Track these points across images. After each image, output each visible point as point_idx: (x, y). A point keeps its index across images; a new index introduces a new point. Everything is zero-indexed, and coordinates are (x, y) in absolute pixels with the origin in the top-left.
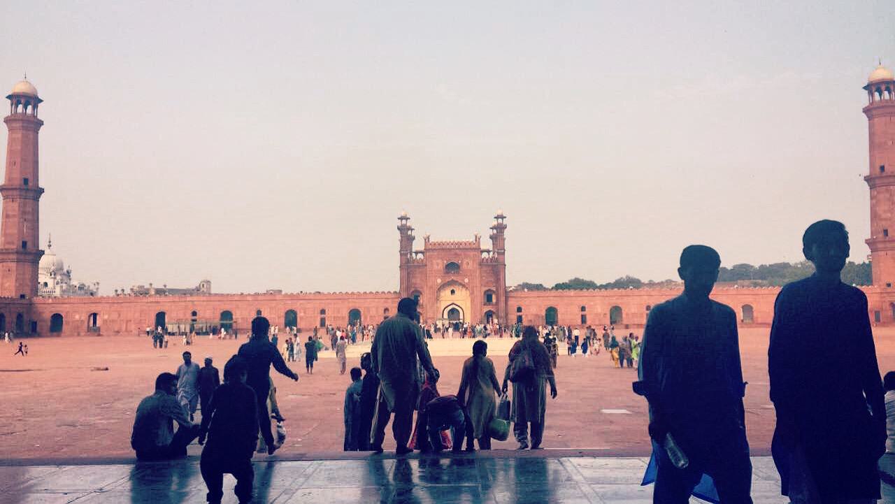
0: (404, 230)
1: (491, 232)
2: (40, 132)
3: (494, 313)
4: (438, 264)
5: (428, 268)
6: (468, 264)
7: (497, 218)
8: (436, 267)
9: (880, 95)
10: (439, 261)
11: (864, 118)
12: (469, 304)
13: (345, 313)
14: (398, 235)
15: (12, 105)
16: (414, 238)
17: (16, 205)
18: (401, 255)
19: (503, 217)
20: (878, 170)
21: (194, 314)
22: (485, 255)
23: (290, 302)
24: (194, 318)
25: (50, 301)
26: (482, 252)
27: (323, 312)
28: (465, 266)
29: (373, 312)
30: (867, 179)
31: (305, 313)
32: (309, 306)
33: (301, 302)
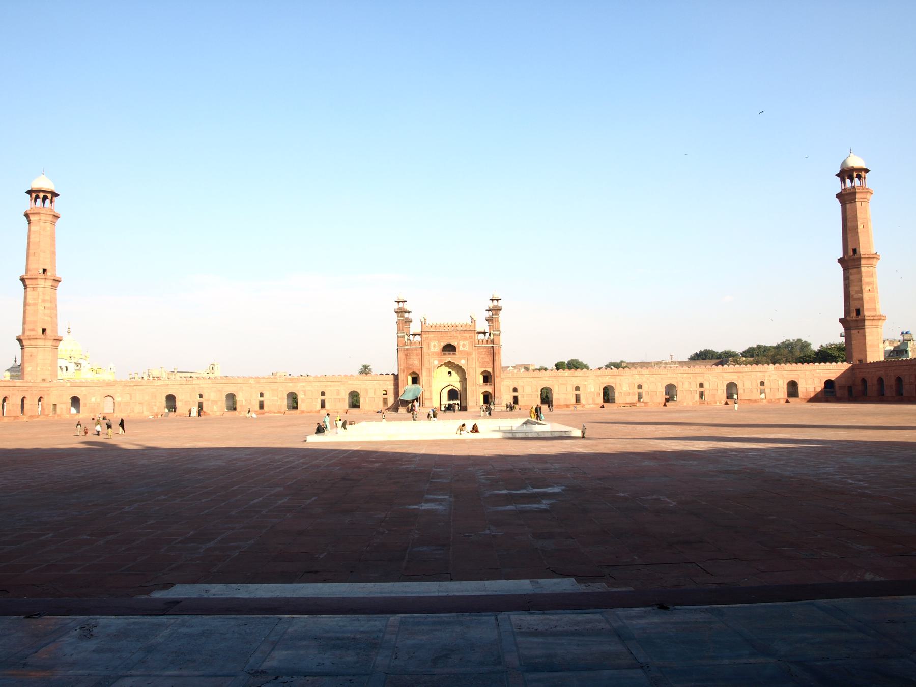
0: (400, 312)
4: (436, 346)
5: (425, 350)
6: (462, 345)
8: (433, 349)
10: (436, 343)
11: (838, 205)
18: (398, 337)
20: (851, 253)
23: (291, 384)
25: (69, 384)
27: (323, 394)
30: (840, 261)
32: (308, 388)
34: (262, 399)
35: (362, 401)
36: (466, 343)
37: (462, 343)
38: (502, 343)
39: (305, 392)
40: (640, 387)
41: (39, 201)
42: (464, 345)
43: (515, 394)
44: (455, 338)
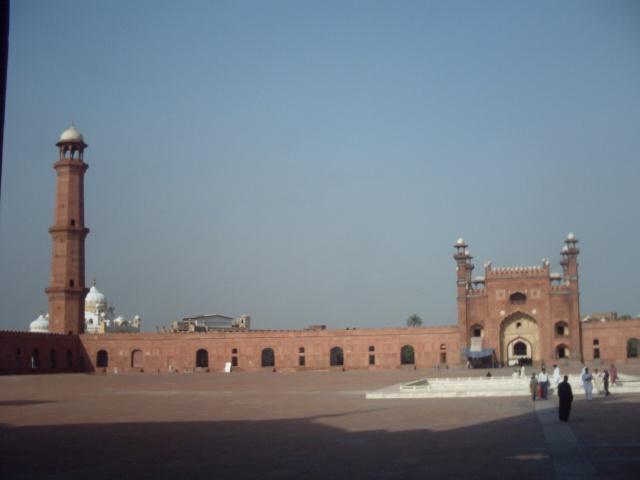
0: (461, 258)
3: (567, 347)
4: (501, 295)
5: (490, 299)
6: (534, 294)
8: (498, 298)
10: (504, 292)
12: (537, 338)
13: (397, 350)
17: (64, 246)
18: (459, 286)
21: (235, 351)
22: (555, 283)
23: (335, 339)
27: (372, 349)
28: (532, 297)
29: (428, 348)
31: (352, 350)
33: (349, 338)
34: (302, 354)
35: (416, 356)
36: (539, 292)
37: (532, 291)
39: (352, 347)
41: (68, 152)
42: (535, 293)
43: (596, 346)
44: (523, 284)
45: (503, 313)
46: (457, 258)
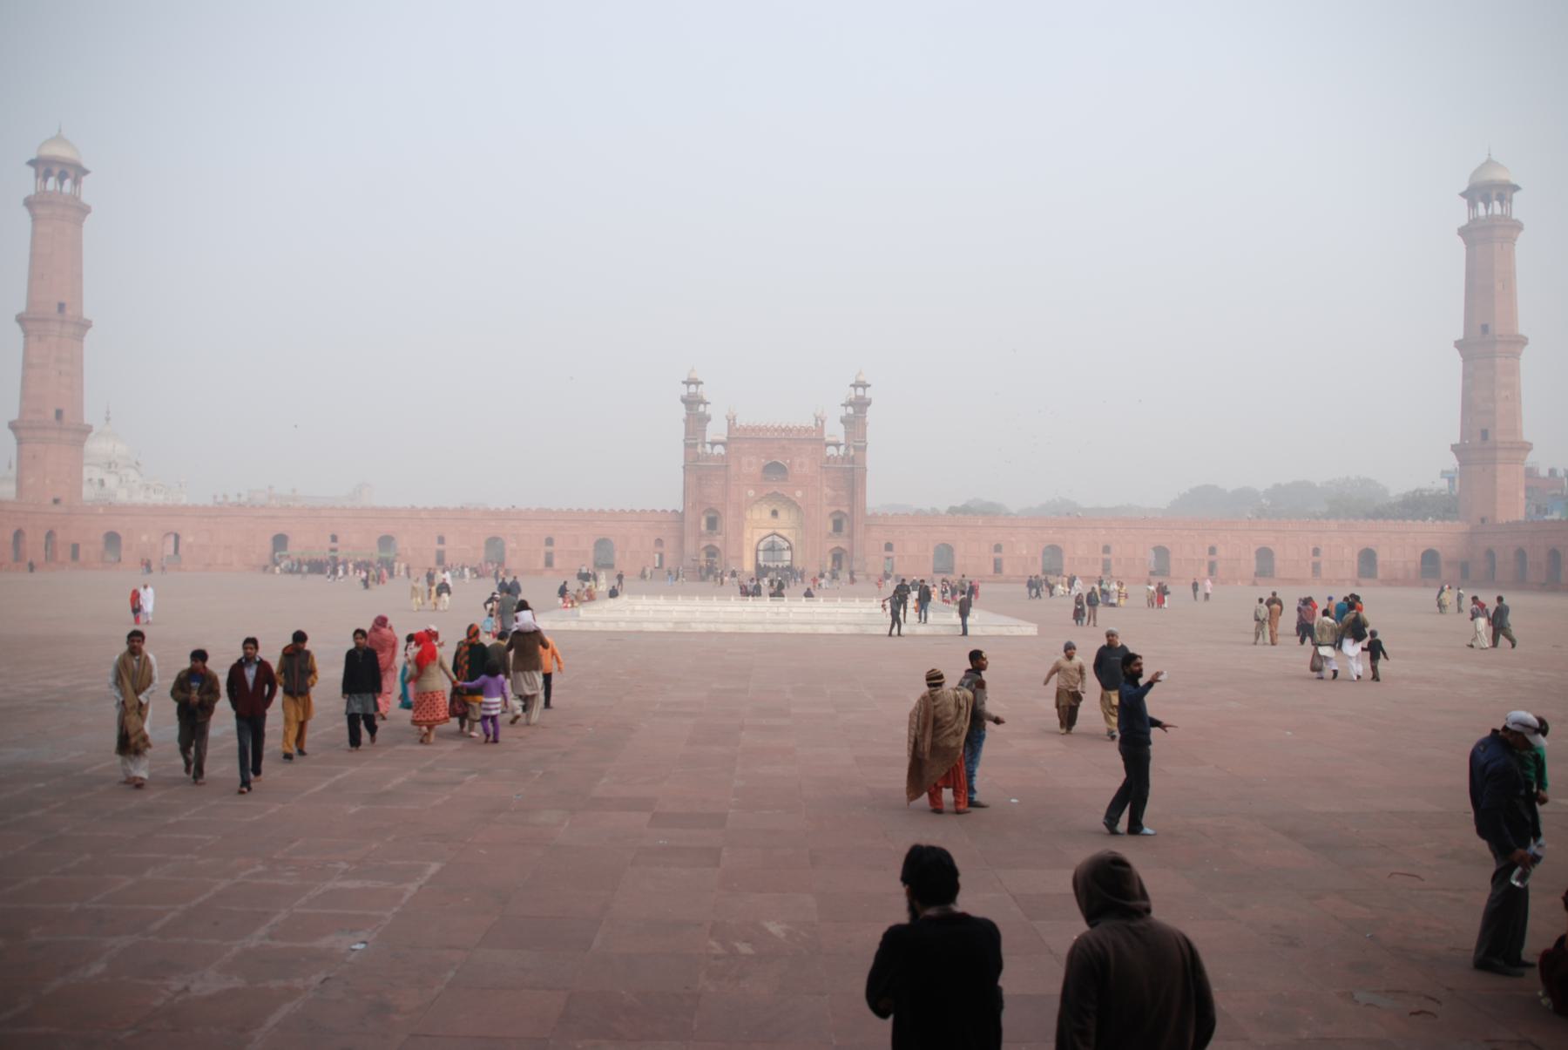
0: (691, 402)
1: (842, 412)
2: (85, 224)
7: (854, 386)
9: (1487, 208)
14: (682, 411)
15: (37, 176)
16: (709, 419)
18: (686, 445)
19: (865, 386)
21: (334, 539)
24: (334, 545)
26: (828, 445)
30: (1458, 344)
34: (441, 547)
35: (617, 555)
38: (869, 464)
40: (1106, 549)
45: (751, 493)
46: (684, 400)
